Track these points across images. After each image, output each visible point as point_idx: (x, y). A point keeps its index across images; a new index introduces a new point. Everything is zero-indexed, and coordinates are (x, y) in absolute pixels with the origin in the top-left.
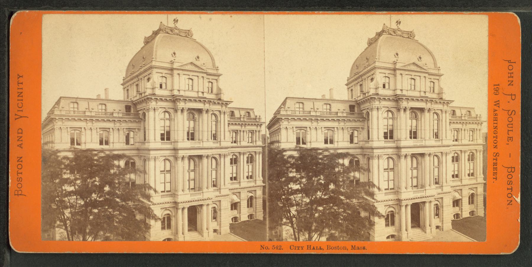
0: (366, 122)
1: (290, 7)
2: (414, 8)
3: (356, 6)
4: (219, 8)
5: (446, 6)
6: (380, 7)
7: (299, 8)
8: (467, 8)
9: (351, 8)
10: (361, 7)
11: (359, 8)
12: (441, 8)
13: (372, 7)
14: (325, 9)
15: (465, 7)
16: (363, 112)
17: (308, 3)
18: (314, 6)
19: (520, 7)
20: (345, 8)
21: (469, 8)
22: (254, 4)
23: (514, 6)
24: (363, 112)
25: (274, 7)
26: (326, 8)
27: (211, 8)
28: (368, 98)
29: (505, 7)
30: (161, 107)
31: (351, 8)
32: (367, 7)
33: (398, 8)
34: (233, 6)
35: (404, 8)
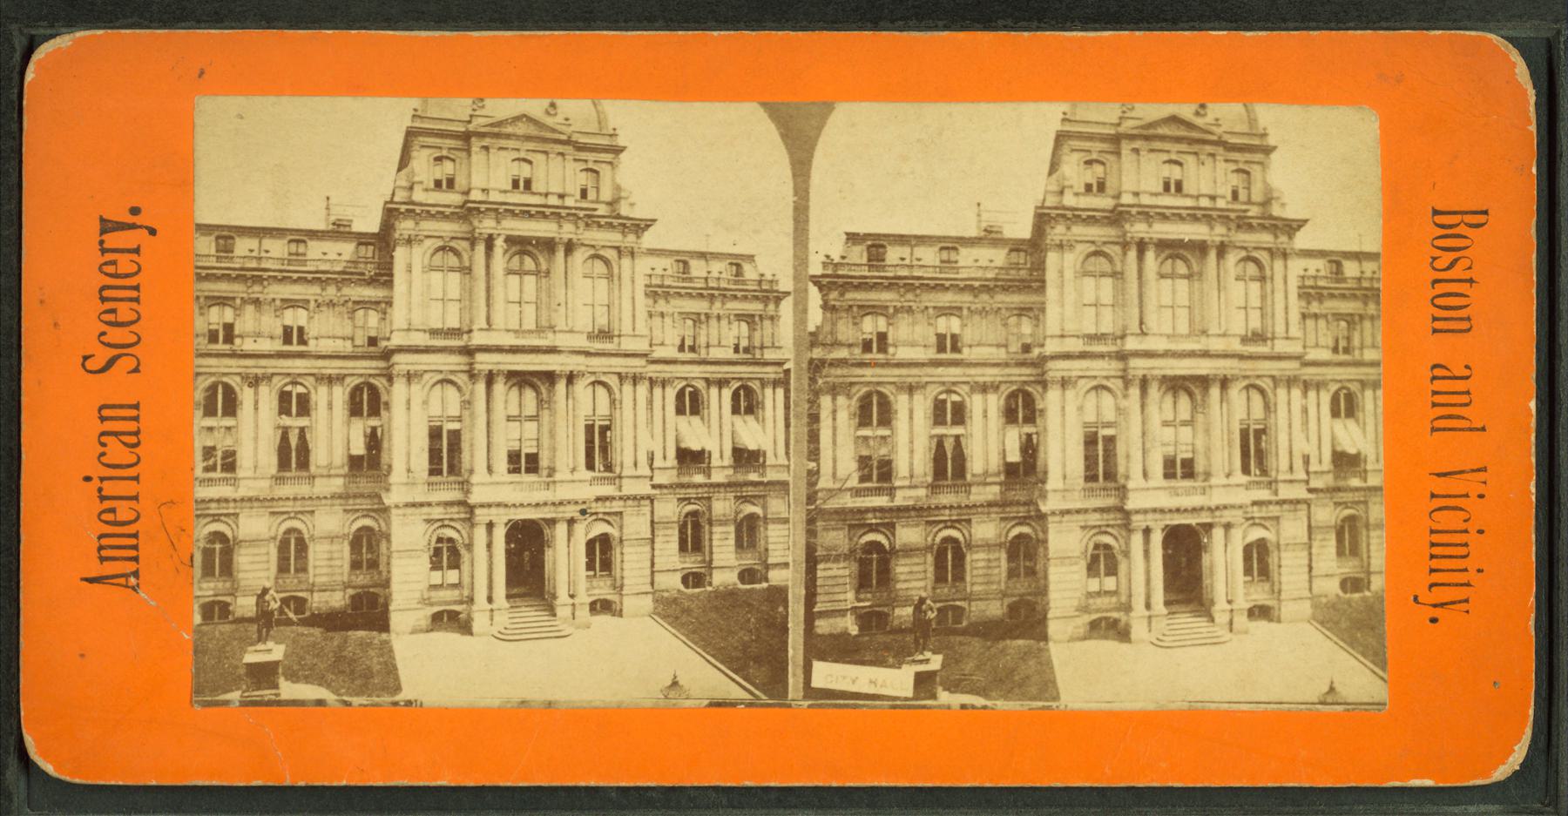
1: (836, 23)
2: (1192, 24)
3: (1024, 20)
5: (1284, 20)
6: (1095, 21)
7: (860, 24)
8: (1347, 25)
10: (1040, 21)
11: (1035, 23)
12: (1270, 25)
14: (936, 26)
15: (1340, 22)
17: (886, 11)
18: (901, 19)
19: (1498, 21)
20: (994, 24)
22: (731, 14)
23: (1483, 19)
27: (605, 24)
29: (1455, 20)
31: (1012, 24)
32: (1057, 23)
33: (1146, 25)
34: (671, 20)
35: (1164, 24)
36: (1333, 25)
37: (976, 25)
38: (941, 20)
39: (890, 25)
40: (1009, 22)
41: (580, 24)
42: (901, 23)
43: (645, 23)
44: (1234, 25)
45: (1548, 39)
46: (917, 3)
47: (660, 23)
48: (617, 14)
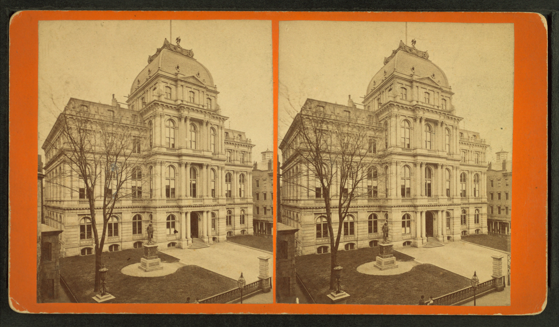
0: (384, 133)
2: (423, 9)
3: (363, 8)
4: (224, 9)
6: (388, 8)
9: (358, 9)
10: (368, 8)
13: (380, 9)
15: (475, 9)
16: (381, 122)
19: (530, 9)
20: (352, 9)
21: (478, 10)
24: (381, 122)
25: (279, 8)
26: (333, 9)
28: (387, 105)
30: (166, 114)
31: (358, 9)
34: (239, 7)
36: (472, 10)
37: (346, 9)
38: (334, 8)
39: (316, 9)
40: (358, 8)
41: (207, 9)
42: (320, 9)
43: (229, 8)
44: (437, 10)
45: (548, 15)
46: (325, 2)
47: (235, 8)
48: (219, 5)
